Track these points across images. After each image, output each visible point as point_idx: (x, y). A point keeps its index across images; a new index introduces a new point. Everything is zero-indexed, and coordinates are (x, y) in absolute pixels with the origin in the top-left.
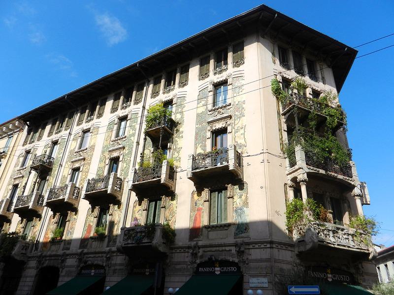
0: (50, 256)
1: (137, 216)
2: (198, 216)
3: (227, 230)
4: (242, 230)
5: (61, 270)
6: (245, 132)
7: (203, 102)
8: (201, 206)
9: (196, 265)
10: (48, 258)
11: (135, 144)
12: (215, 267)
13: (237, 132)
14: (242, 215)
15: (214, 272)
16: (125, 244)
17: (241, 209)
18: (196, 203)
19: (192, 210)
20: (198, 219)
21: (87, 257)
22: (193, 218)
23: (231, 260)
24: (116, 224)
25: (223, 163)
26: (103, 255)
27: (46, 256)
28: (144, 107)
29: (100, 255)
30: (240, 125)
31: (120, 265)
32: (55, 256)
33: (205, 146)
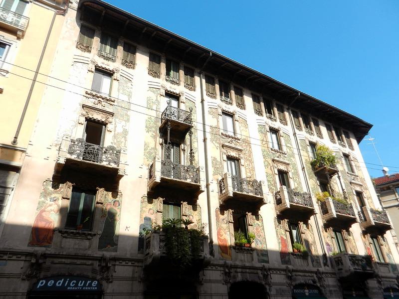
0: (244, 267)
5: (267, 287)
10: (239, 270)
12: (305, 289)
15: (305, 293)
21: (296, 275)
24: (312, 244)
26: (313, 274)
27: (236, 267)
29: (310, 274)
31: (334, 286)
32: (250, 268)
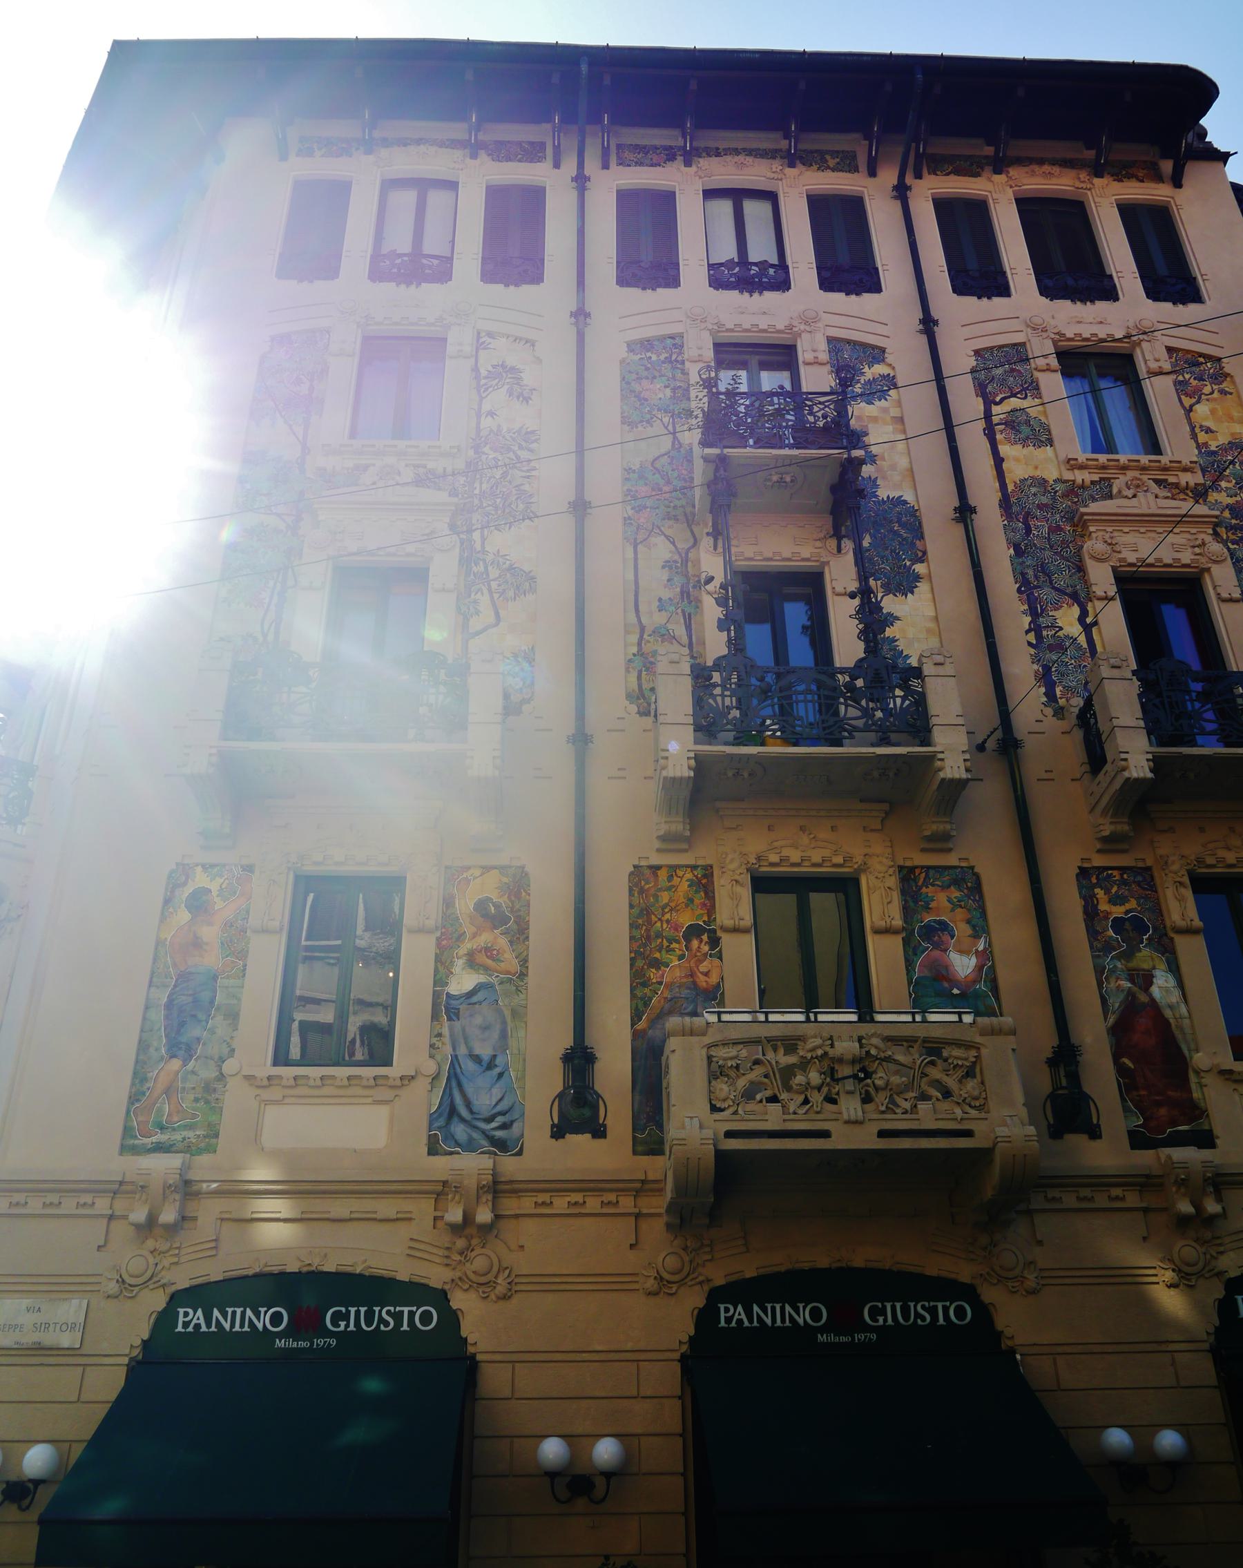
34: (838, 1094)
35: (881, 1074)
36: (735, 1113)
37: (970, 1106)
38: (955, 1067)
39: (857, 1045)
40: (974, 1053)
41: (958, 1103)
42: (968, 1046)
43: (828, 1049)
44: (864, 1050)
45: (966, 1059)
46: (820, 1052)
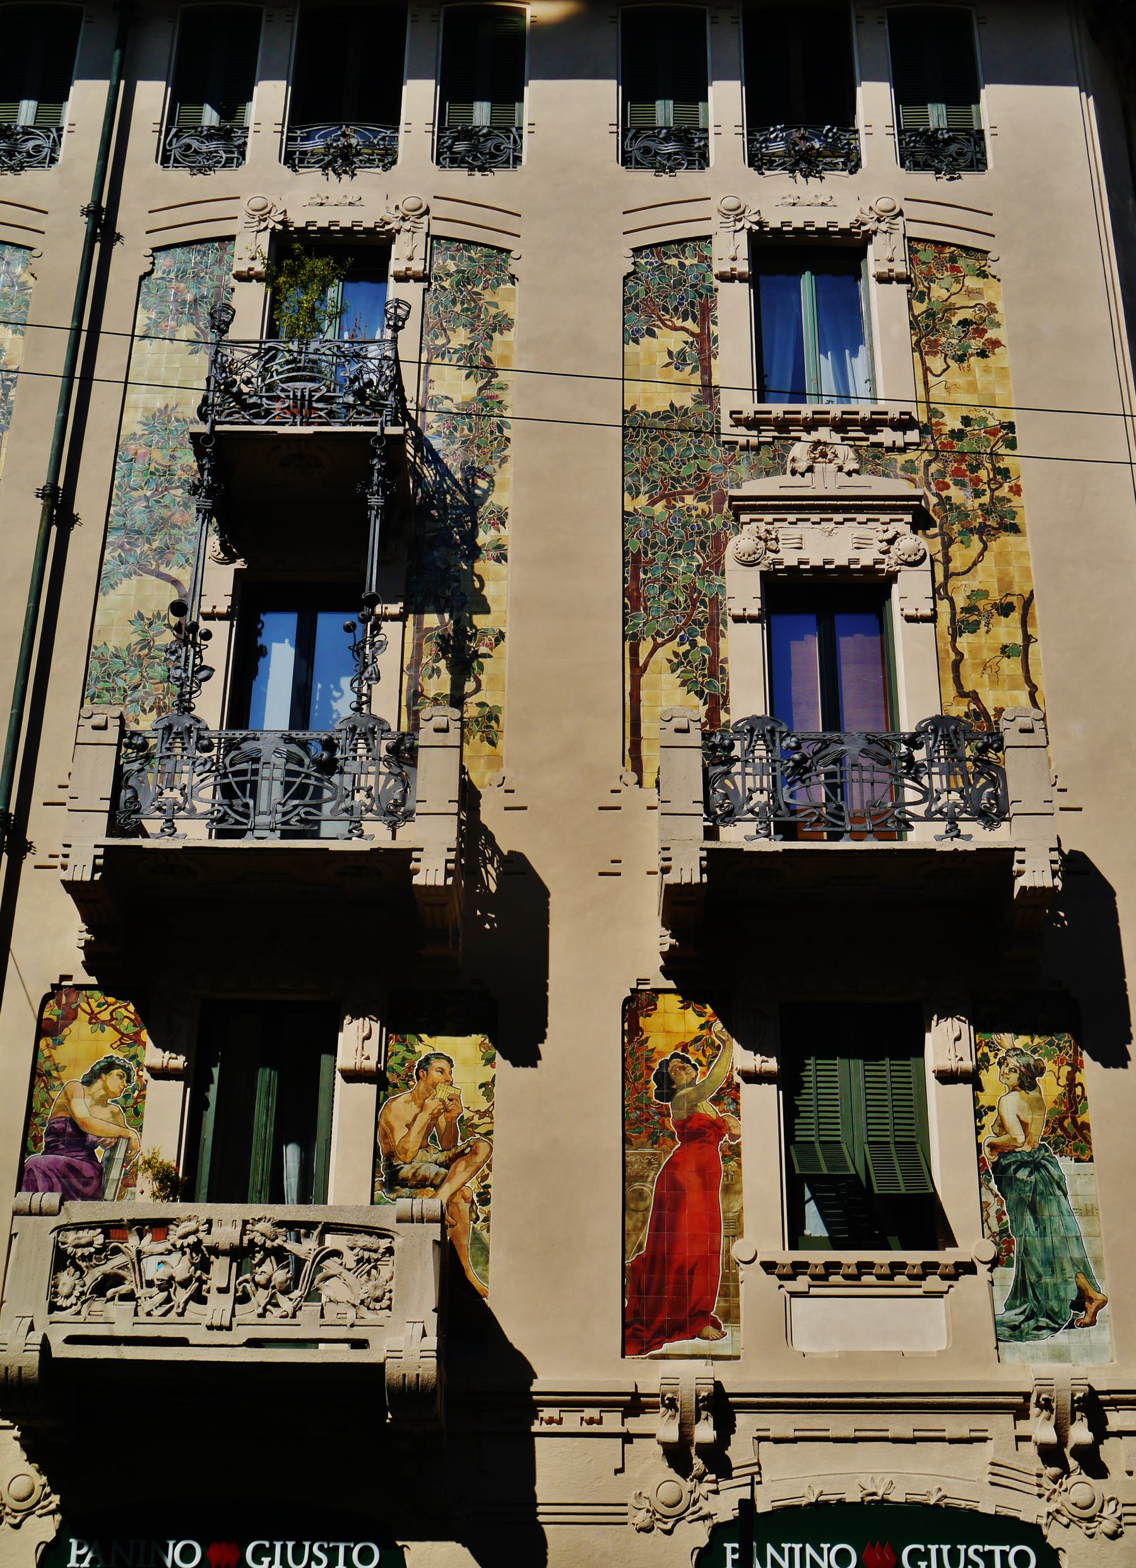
1: (81, 1109)
2: (689, 1177)
3: (939, 1295)
4: (1054, 1304)
6: (1028, 639)
7: (674, 341)
8: (707, 1109)
9: (699, 1535)
11: (88, 501)
13: (974, 628)
14: (1049, 1210)
16: (71, 1340)
17: (1036, 1166)
18: (667, 1087)
19: (636, 1126)
20: (693, 1198)
22: (650, 1189)
23: (987, 1507)
25: (964, 827)
28: (102, 225)
30: (985, 578)
33: (715, 668)
34: (208, 1291)
35: (267, 1267)
36: (78, 1313)
37: (369, 1309)
38: (359, 1261)
39: (239, 1229)
40: (384, 1243)
41: (354, 1306)
42: (382, 1233)
43: (201, 1235)
44: (246, 1239)
45: (376, 1251)
46: (192, 1239)
